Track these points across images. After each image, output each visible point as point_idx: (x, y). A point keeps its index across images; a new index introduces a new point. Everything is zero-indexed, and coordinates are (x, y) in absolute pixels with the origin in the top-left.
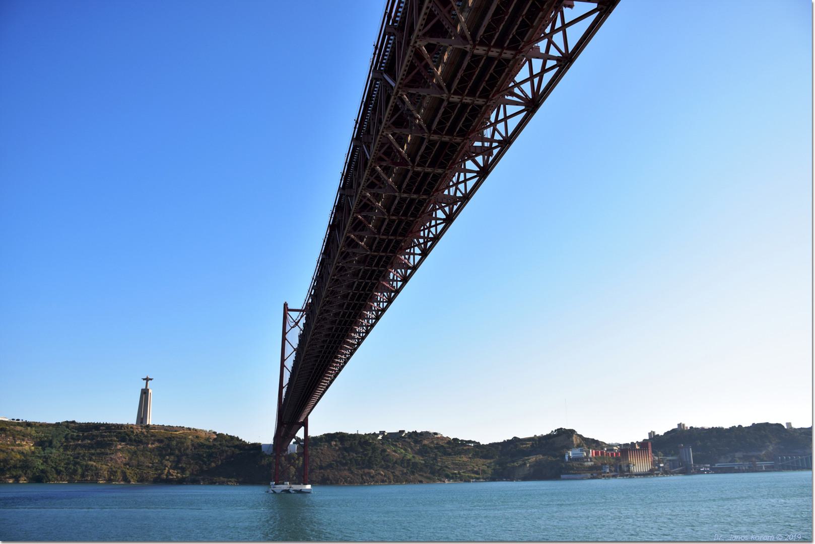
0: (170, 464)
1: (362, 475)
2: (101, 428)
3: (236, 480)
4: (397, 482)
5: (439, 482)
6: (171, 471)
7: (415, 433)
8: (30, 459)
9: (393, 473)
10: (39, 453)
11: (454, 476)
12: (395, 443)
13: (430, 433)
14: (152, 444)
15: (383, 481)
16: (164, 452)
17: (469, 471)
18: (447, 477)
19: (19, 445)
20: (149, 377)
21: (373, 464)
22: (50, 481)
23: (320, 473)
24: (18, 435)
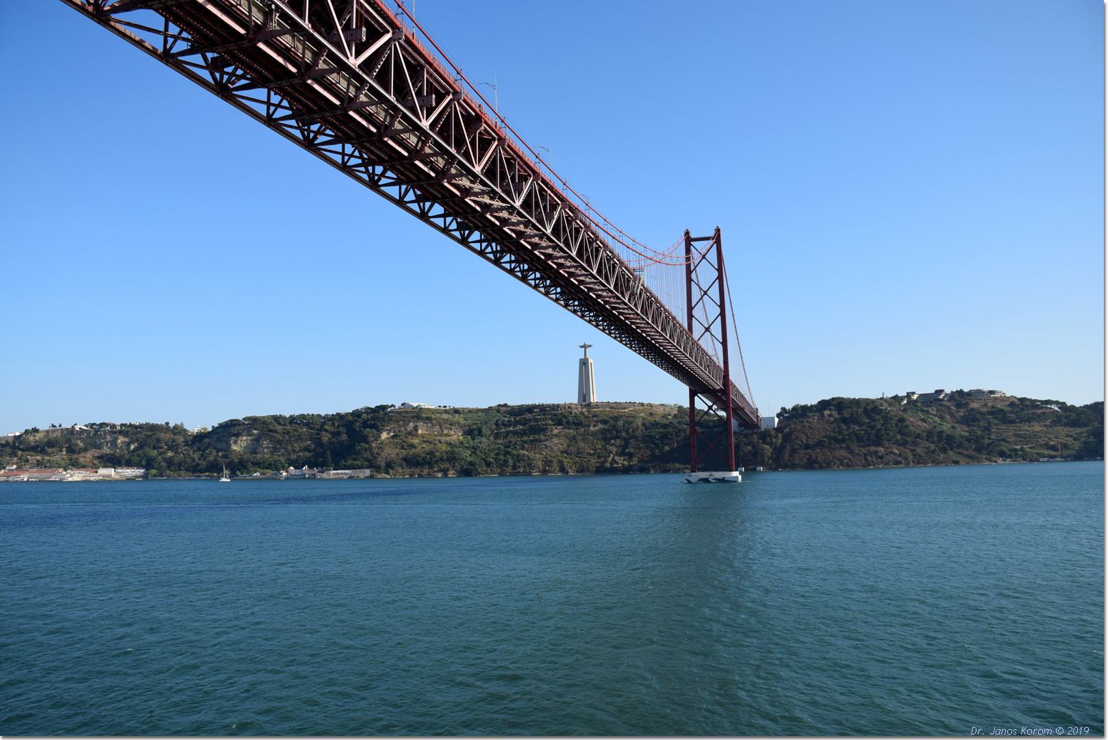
0: (615, 450)
1: (865, 455)
2: (535, 410)
4: (919, 463)
5: (988, 463)
6: (616, 458)
7: (960, 392)
8: (456, 450)
9: (911, 450)
10: (468, 443)
11: (1013, 454)
12: (926, 409)
13: (983, 392)
14: (594, 426)
15: (897, 463)
16: (609, 436)
17: (1041, 445)
18: (1003, 455)
19: (447, 435)
20: (587, 343)
21: (882, 440)
22: (479, 474)
23: (805, 453)
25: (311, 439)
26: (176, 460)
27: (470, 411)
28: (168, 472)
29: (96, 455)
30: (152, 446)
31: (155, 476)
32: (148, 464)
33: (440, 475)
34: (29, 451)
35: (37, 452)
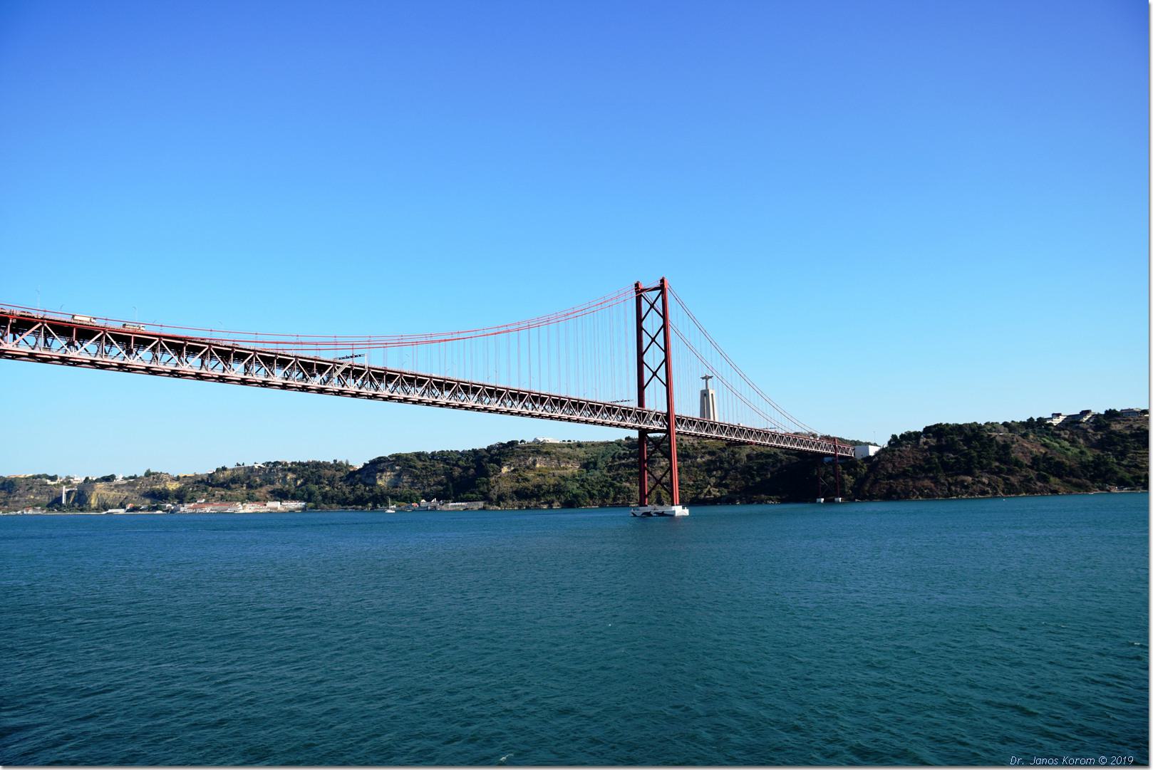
1: (950, 484)
3: (779, 497)
9: (1005, 479)
12: (1058, 432)
14: (702, 457)
15: (983, 493)
19: (563, 468)
22: (581, 506)
23: (887, 484)
24: (564, 457)
25: (445, 474)
26: (330, 494)
27: (593, 445)
28: (323, 505)
29: (270, 490)
30: (315, 481)
31: (311, 508)
32: (308, 497)
33: (545, 507)
34: (217, 487)
35: (224, 488)
